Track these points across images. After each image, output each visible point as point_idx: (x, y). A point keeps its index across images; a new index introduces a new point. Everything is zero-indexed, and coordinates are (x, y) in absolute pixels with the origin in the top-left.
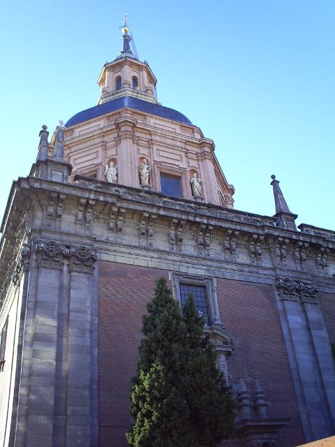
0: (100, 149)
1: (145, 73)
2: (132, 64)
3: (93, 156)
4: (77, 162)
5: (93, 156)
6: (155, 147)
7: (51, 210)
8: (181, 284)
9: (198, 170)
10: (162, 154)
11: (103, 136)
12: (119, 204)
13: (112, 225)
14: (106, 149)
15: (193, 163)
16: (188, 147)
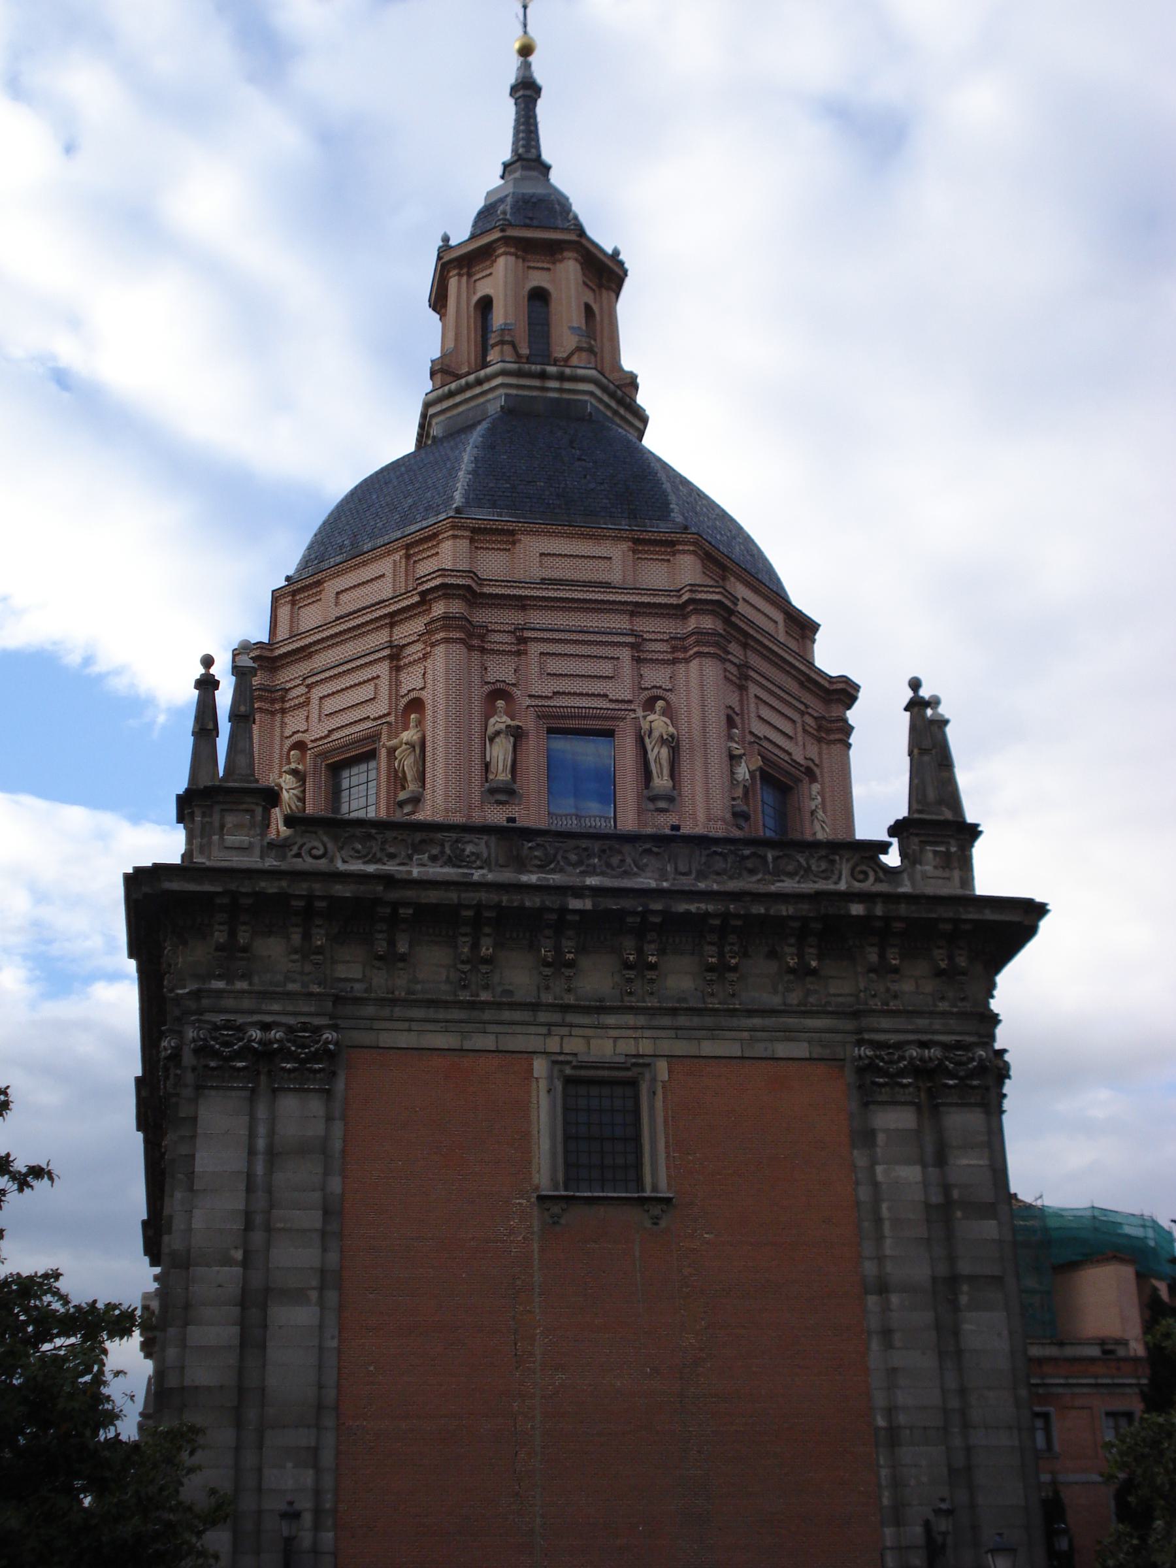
0: (383, 669)
1: (569, 270)
2: (526, 249)
3: (366, 692)
4: (331, 705)
5: (366, 692)
6: (534, 649)
7: (220, 936)
8: (568, 1081)
9: (671, 696)
10: (554, 666)
11: (392, 625)
12: (394, 895)
13: (381, 947)
14: (398, 669)
15: (655, 676)
16: (648, 626)
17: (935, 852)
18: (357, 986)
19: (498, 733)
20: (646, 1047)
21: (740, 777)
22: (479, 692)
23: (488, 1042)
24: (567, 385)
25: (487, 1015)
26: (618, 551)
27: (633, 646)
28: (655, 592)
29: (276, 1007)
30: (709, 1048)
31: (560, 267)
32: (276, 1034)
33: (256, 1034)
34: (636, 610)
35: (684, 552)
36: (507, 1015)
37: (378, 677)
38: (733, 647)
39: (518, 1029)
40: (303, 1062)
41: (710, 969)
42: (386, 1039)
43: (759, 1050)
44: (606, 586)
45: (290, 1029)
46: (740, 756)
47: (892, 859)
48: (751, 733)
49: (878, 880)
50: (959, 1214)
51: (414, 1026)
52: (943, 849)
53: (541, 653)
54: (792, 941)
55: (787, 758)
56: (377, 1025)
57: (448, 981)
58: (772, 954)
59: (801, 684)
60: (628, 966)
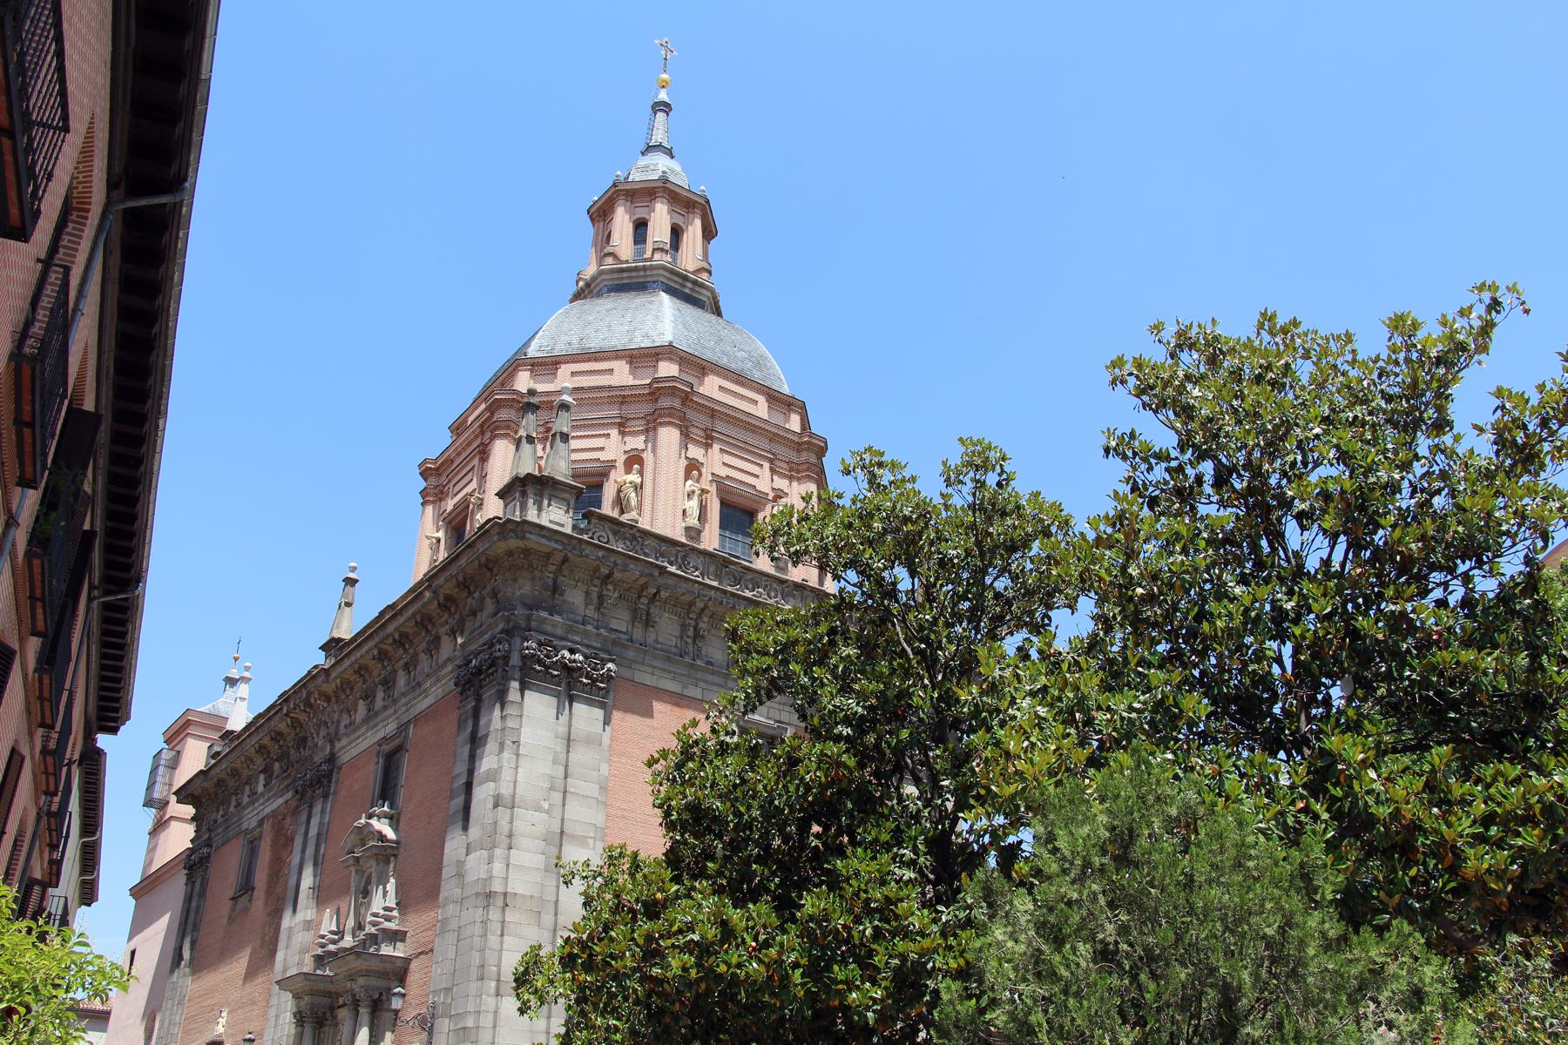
6: (716, 447)
11: (622, 403)
15: (781, 483)
18: (623, 636)
19: (693, 492)
22: (684, 463)
24: (697, 289)
25: (699, 675)
26: (761, 399)
27: (771, 461)
31: (691, 216)
33: (567, 654)
35: (795, 412)
36: (710, 678)
39: (715, 688)
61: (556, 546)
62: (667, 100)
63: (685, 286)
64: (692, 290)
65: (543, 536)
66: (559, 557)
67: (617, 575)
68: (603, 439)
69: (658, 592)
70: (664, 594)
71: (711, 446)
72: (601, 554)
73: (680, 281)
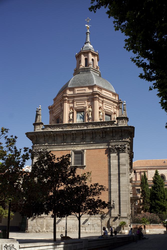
0: (60, 107)
5: (59, 110)
6: (75, 102)
10: (77, 104)
11: (61, 101)
17: (121, 121)
20: (84, 148)
21: (101, 114)
23: (65, 149)
24: (88, 69)
26: (87, 89)
28: (89, 93)
29: (42, 147)
30: (91, 148)
32: (41, 150)
34: (87, 96)
37: (60, 108)
38: (100, 98)
40: (44, 153)
41: (91, 138)
42: (54, 150)
43: (97, 148)
44: (85, 93)
45: (43, 149)
46: (101, 112)
47: (116, 123)
48: (104, 109)
49: (114, 125)
50: (121, 166)
51: (57, 148)
52: (122, 120)
53: (76, 103)
54: (102, 134)
55: (110, 112)
56: (53, 148)
57: (61, 142)
58: (100, 136)
59: (113, 102)
60: (81, 139)
61: (33, 134)
62: (89, 32)
63: (85, 70)
64: (87, 70)
65: (31, 134)
66: (35, 136)
67: (45, 135)
68: (59, 109)
69: (54, 135)
70: (55, 135)
71: (74, 103)
72: (41, 133)
73: (84, 69)
